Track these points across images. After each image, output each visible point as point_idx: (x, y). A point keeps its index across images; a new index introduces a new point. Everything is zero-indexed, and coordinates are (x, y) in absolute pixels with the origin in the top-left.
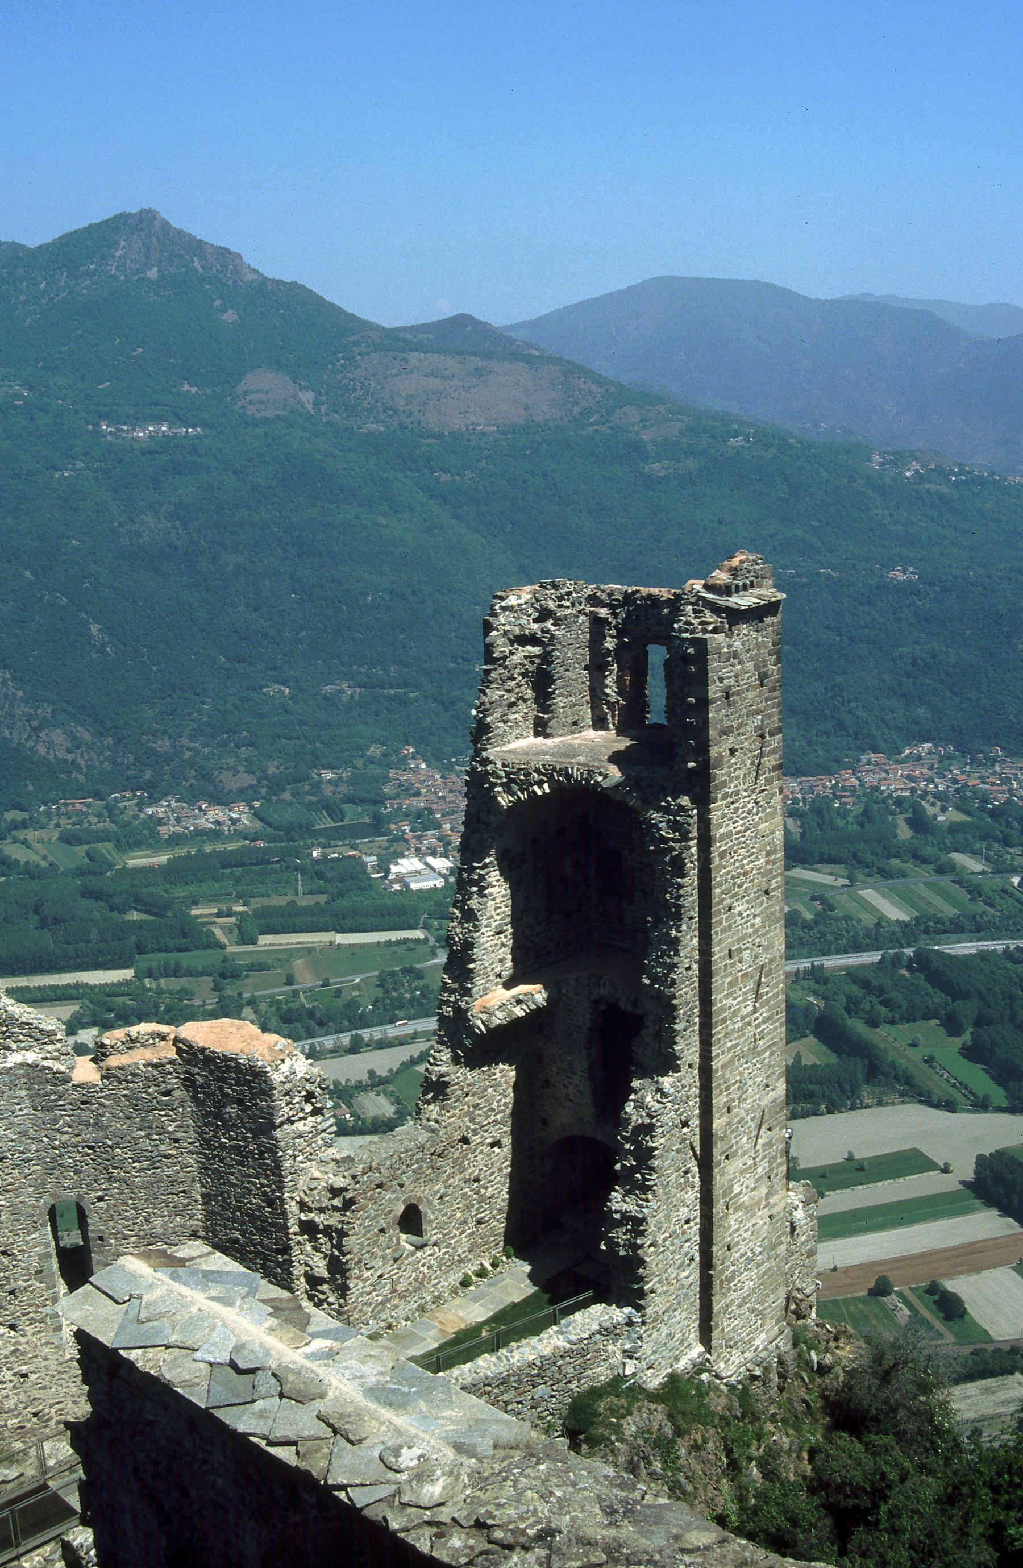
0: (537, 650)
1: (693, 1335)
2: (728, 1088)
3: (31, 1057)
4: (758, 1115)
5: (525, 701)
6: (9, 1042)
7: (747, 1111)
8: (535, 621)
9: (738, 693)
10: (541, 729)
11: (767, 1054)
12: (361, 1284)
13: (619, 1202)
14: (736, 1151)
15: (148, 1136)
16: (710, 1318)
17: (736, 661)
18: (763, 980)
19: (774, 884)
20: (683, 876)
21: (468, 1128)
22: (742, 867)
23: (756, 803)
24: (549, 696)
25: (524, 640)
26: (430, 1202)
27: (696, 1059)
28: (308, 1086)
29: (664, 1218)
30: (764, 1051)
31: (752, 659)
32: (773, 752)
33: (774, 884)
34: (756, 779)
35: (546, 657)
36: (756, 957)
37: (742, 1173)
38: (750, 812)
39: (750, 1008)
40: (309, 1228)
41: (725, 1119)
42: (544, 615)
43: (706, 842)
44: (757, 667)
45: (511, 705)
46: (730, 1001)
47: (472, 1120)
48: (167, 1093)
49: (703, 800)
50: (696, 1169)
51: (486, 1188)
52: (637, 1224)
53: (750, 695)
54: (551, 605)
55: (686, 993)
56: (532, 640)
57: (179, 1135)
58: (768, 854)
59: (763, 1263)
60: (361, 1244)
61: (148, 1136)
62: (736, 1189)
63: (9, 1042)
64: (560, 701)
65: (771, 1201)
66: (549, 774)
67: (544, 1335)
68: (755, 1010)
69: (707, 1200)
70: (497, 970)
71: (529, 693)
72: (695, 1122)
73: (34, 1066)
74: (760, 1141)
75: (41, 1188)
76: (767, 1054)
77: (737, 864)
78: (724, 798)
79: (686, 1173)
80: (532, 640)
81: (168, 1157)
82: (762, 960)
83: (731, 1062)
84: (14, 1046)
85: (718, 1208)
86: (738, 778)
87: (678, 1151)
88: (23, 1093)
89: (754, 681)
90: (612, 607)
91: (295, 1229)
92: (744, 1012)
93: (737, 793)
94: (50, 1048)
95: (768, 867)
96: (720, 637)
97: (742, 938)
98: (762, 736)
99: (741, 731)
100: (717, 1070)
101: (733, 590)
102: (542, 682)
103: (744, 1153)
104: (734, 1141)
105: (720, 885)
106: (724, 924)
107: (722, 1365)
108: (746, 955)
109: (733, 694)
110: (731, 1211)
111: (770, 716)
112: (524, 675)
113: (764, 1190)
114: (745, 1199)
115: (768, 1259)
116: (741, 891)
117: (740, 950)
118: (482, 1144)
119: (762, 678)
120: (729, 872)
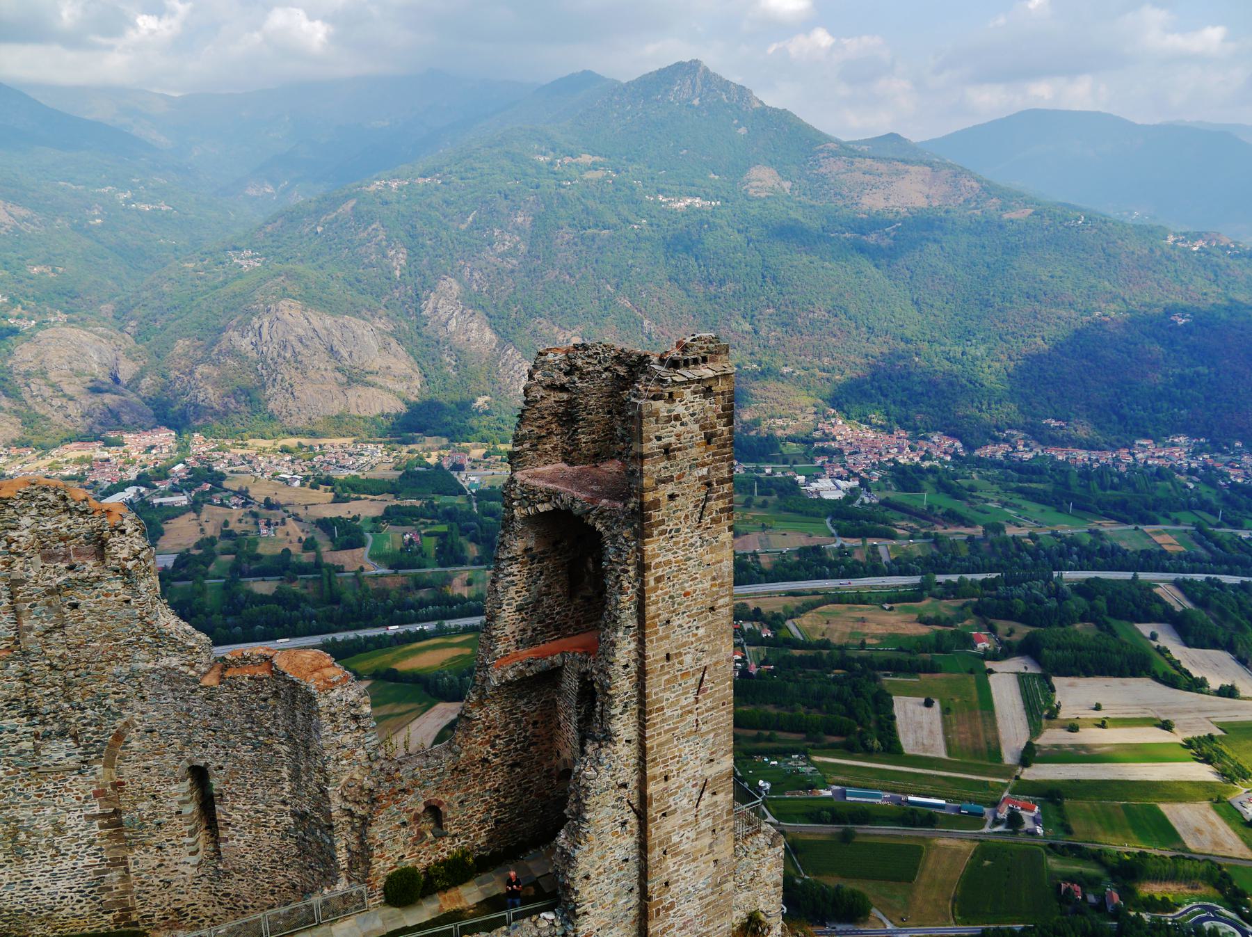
0: (565, 396)
2: (667, 761)
3: (175, 661)
4: (701, 783)
7: (688, 780)
9: (679, 449)
11: (712, 735)
12: (382, 862)
13: (562, 838)
14: (675, 810)
15: (251, 729)
17: (678, 423)
18: (706, 677)
19: (721, 602)
20: (621, 594)
21: (488, 752)
25: (552, 387)
26: (449, 805)
28: (353, 711)
30: (709, 732)
31: (697, 421)
32: (718, 498)
33: (721, 602)
34: (700, 518)
36: (699, 660)
37: (681, 827)
38: (692, 545)
39: (693, 700)
41: (663, 785)
43: (642, 568)
44: (703, 428)
46: (667, 695)
47: (493, 747)
48: (265, 700)
49: (642, 535)
51: (506, 798)
52: (569, 859)
53: (694, 452)
54: (579, 363)
55: (623, 685)
56: (562, 388)
57: (273, 730)
58: (714, 579)
59: (706, 896)
60: (384, 832)
61: (251, 729)
62: (675, 839)
66: (550, 495)
67: (494, 933)
68: (697, 701)
69: (643, 847)
70: (518, 638)
72: (632, 785)
74: (702, 803)
75: (180, 755)
76: (712, 735)
77: (677, 586)
78: (661, 534)
79: (624, 824)
80: (562, 388)
81: (266, 745)
82: (706, 661)
84: (164, 653)
85: (654, 855)
87: (613, 807)
88: (166, 687)
90: (630, 367)
92: (684, 702)
93: (678, 530)
95: (714, 589)
96: (659, 404)
97: (683, 645)
98: (709, 485)
100: (652, 748)
103: (685, 812)
104: (672, 803)
106: (661, 633)
108: (688, 659)
109: (674, 450)
110: (669, 856)
111: (717, 469)
112: (555, 415)
113: (707, 840)
114: (685, 846)
115: (712, 893)
116: (682, 609)
117: (680, 654)
119: (709, 439)
120: (666, 593)
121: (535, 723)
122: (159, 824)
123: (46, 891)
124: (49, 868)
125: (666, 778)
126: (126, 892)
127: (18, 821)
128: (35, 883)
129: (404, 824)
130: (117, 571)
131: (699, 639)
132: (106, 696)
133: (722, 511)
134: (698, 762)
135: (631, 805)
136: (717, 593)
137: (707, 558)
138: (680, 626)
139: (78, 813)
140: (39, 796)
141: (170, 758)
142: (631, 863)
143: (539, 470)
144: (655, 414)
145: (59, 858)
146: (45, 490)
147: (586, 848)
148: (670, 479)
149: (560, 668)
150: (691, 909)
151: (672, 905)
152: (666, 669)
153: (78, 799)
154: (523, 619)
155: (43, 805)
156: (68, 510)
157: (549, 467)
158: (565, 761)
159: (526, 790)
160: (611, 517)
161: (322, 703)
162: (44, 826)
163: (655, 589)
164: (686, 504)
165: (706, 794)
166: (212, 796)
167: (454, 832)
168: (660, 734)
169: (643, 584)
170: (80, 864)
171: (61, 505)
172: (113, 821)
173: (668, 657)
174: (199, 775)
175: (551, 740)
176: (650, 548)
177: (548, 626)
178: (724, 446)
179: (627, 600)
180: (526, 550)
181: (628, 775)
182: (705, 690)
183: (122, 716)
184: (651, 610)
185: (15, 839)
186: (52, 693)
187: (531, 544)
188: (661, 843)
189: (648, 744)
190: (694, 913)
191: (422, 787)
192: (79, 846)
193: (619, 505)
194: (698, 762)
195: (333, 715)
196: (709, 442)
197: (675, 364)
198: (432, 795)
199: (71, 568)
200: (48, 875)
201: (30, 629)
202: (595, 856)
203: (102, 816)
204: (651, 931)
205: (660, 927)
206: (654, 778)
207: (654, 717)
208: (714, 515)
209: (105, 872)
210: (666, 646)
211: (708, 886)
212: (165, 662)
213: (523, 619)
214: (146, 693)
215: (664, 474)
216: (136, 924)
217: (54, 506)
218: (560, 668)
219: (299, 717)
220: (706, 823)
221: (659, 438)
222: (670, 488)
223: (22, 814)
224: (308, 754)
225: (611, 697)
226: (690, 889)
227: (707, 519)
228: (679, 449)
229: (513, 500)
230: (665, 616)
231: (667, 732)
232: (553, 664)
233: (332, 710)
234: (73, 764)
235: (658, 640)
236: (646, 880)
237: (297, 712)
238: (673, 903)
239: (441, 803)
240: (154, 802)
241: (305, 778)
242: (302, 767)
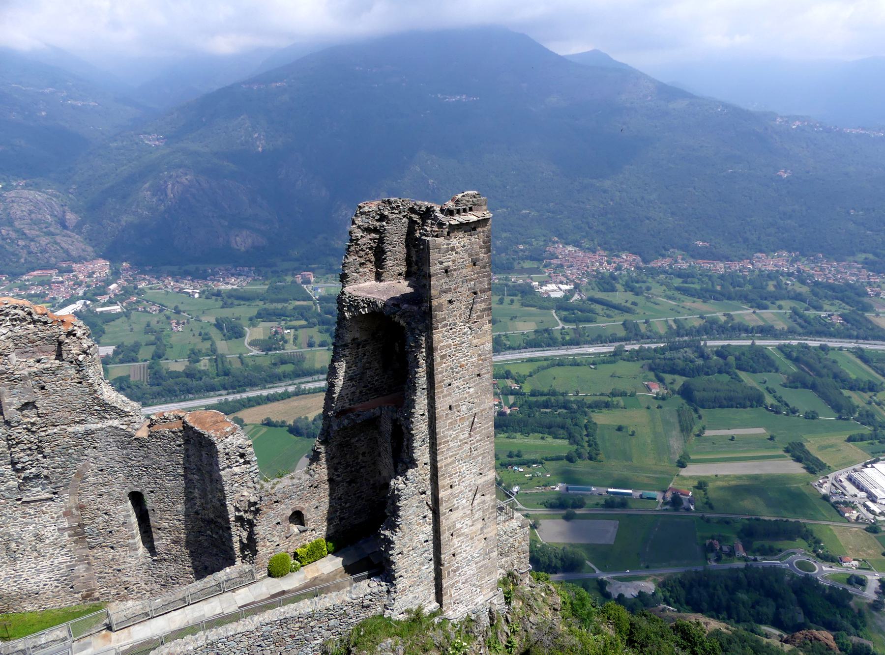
0: (377, 236)
1: (433, 596)
3: (116, 423)
4: (474, 489)
5: (371, 262)
6: (106, 415)
7: (466, 487)
8: (377, 220)
9: (455, 270)
10: (379, 277)
14: (458, 507)
16: (441, 590)
20: (418, 367)
22: (459, 363)
23: (470, 328)
24: (384, 260)
25: (368, 230)
27: (428, 460)
29: (409, 540)
30: (479, 456)
31: (466, 251)
33: (484, 371)
35: (381, 241)
36: (471, 409)
38: (464, 334)
39: (467, 435)
40: (239, 519)
41: (450, 491)
42: (383, 218)
43: (431, 350)
44: (470, 255)
45: (361, 264)
46: (451, 432)
50: (431, 515)
53: (465, 271)
54: (386, 213)
58: (480, 355)
60: (265, 530)
62: (458, 526)
63: (106, 415)
64: (389, 263)
65: (485, 531)
67: (341, 592)
68: (470, 435)
71: (373, 259)
72: (429, 493)
73: (116, 428)
78: (444, 327)
80: (375, 230)
83: (453, 462)
85: (445, 536)
86: (455, 316)
88: (111, 440)
89: (468, 262)
91: (233, 519)
92: (462, 437)
93: (455, 324)
94: (126, 419)
99: (459, 290)
101: (455, 212)
102: (379, 254)
105: (441, 373)
106: (445, 392)
107: (451, 613)
108: (464, 408)
112: (371, 249)
113: (479, 525)
114: (466, 531)
116: (459, 376)
118: (342, 481)
121: (364, 454)
122: (111, 532)
123: (33, 581)
124: (34, 566)
125: (451, 487)
126: (90, 578)
127: (10, 536)
128: (25, 576)
129: (278, 523)
130: (72, 362)
131: (471, 396)
132: (67, 448)
133: (484, 310)
134: (472, 476)
135: (428, 505)
136: (482, 364)
137: (475, 341)
138: (458, 387)
139: (53, 527)
140: (24, 518)
141: (116, 488)
142: (430, 542)
143: (362, 285)
144: (438, 248)
145: (41, 559)
146: (15, 308)
147: (400, 534)
148: (449, 290)
149: (379, 417)
150: (470, 571)
151: (458, 568)
152: (450, 416)
153: (52, 518)
154: (353, 385)
155: (27, 524)
156: (34, 322)
157: (368, 283)
158: (384, 478)
159: (359, 497)
160: (410, 316)
161: (219, 447)
162: (28, 537)
163: (441, 363)
164: (461, 307)
165: (478, 496)
166: (147, 511)
167: (312, 527)
168: (446, 458)
169: (433, 360)
170: (56, 562)
171: (28, 318)
172: (79, 534)
173: (450, 407)
174: (137, 498)
175: (374, 464)
176: (437, 336)
177: (370, 389)
178: (485, 267)
179: (422, 371)
180: (354, 340)
181: (427, 486)
182: (476, 428)
183: (80, 461)
184: (438, 378)
185: (8, 549)
186: (30, 449)
187: (357, 335)
188: (449, 529)
189: (439, 465)
190: (472, 572)
191: (290, 498)
192: (54, 549)
193: (416, 308)
194: (472, 476)
195: (227, 454)
196: (474, 265)
197: (450, 213)
198: (298, 505)
199: (38, 361)
200: (33, 570)
201: (11, 404)
202: (406, 539)
203: (70, 528)
204: (444, 586)
205: (451, 582)
206: (444, 487)
207: (441, 448)
208: (479, 313)
209: (74, 566)
210: (449, 401)
211: (481, 555)
212: (110, 423)
213: (353, 385)
214: (96, 445)
215: (445, 287)
216: (98, 599)
217: (24, 319)
218: (379, 417)
219: (204, 456)
220: (478, 515)
221: (441, 263)
222: (449, 296)
223: (12, 531)
224: (211, 481)
225: (413, 435)
226: (469, 557)
227: (474, 315)
228: (455, 270)
229: (344, 306)
230: (448, 381)
231: (451, 457)
232: (374, 414)
233: (227, 451)
234: (48, 496)
235: (443, 397)
236: (440, 553)
237: (203, 453)
238: (458, 567)
239: (302, 508)
240: (107, 517)
241: (210, 496)
242: (208, 489)
